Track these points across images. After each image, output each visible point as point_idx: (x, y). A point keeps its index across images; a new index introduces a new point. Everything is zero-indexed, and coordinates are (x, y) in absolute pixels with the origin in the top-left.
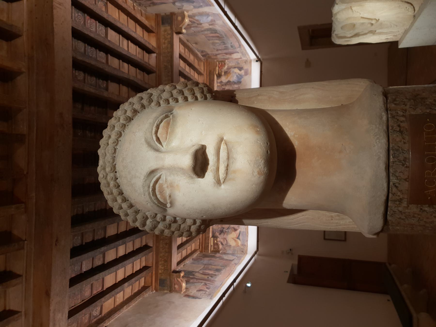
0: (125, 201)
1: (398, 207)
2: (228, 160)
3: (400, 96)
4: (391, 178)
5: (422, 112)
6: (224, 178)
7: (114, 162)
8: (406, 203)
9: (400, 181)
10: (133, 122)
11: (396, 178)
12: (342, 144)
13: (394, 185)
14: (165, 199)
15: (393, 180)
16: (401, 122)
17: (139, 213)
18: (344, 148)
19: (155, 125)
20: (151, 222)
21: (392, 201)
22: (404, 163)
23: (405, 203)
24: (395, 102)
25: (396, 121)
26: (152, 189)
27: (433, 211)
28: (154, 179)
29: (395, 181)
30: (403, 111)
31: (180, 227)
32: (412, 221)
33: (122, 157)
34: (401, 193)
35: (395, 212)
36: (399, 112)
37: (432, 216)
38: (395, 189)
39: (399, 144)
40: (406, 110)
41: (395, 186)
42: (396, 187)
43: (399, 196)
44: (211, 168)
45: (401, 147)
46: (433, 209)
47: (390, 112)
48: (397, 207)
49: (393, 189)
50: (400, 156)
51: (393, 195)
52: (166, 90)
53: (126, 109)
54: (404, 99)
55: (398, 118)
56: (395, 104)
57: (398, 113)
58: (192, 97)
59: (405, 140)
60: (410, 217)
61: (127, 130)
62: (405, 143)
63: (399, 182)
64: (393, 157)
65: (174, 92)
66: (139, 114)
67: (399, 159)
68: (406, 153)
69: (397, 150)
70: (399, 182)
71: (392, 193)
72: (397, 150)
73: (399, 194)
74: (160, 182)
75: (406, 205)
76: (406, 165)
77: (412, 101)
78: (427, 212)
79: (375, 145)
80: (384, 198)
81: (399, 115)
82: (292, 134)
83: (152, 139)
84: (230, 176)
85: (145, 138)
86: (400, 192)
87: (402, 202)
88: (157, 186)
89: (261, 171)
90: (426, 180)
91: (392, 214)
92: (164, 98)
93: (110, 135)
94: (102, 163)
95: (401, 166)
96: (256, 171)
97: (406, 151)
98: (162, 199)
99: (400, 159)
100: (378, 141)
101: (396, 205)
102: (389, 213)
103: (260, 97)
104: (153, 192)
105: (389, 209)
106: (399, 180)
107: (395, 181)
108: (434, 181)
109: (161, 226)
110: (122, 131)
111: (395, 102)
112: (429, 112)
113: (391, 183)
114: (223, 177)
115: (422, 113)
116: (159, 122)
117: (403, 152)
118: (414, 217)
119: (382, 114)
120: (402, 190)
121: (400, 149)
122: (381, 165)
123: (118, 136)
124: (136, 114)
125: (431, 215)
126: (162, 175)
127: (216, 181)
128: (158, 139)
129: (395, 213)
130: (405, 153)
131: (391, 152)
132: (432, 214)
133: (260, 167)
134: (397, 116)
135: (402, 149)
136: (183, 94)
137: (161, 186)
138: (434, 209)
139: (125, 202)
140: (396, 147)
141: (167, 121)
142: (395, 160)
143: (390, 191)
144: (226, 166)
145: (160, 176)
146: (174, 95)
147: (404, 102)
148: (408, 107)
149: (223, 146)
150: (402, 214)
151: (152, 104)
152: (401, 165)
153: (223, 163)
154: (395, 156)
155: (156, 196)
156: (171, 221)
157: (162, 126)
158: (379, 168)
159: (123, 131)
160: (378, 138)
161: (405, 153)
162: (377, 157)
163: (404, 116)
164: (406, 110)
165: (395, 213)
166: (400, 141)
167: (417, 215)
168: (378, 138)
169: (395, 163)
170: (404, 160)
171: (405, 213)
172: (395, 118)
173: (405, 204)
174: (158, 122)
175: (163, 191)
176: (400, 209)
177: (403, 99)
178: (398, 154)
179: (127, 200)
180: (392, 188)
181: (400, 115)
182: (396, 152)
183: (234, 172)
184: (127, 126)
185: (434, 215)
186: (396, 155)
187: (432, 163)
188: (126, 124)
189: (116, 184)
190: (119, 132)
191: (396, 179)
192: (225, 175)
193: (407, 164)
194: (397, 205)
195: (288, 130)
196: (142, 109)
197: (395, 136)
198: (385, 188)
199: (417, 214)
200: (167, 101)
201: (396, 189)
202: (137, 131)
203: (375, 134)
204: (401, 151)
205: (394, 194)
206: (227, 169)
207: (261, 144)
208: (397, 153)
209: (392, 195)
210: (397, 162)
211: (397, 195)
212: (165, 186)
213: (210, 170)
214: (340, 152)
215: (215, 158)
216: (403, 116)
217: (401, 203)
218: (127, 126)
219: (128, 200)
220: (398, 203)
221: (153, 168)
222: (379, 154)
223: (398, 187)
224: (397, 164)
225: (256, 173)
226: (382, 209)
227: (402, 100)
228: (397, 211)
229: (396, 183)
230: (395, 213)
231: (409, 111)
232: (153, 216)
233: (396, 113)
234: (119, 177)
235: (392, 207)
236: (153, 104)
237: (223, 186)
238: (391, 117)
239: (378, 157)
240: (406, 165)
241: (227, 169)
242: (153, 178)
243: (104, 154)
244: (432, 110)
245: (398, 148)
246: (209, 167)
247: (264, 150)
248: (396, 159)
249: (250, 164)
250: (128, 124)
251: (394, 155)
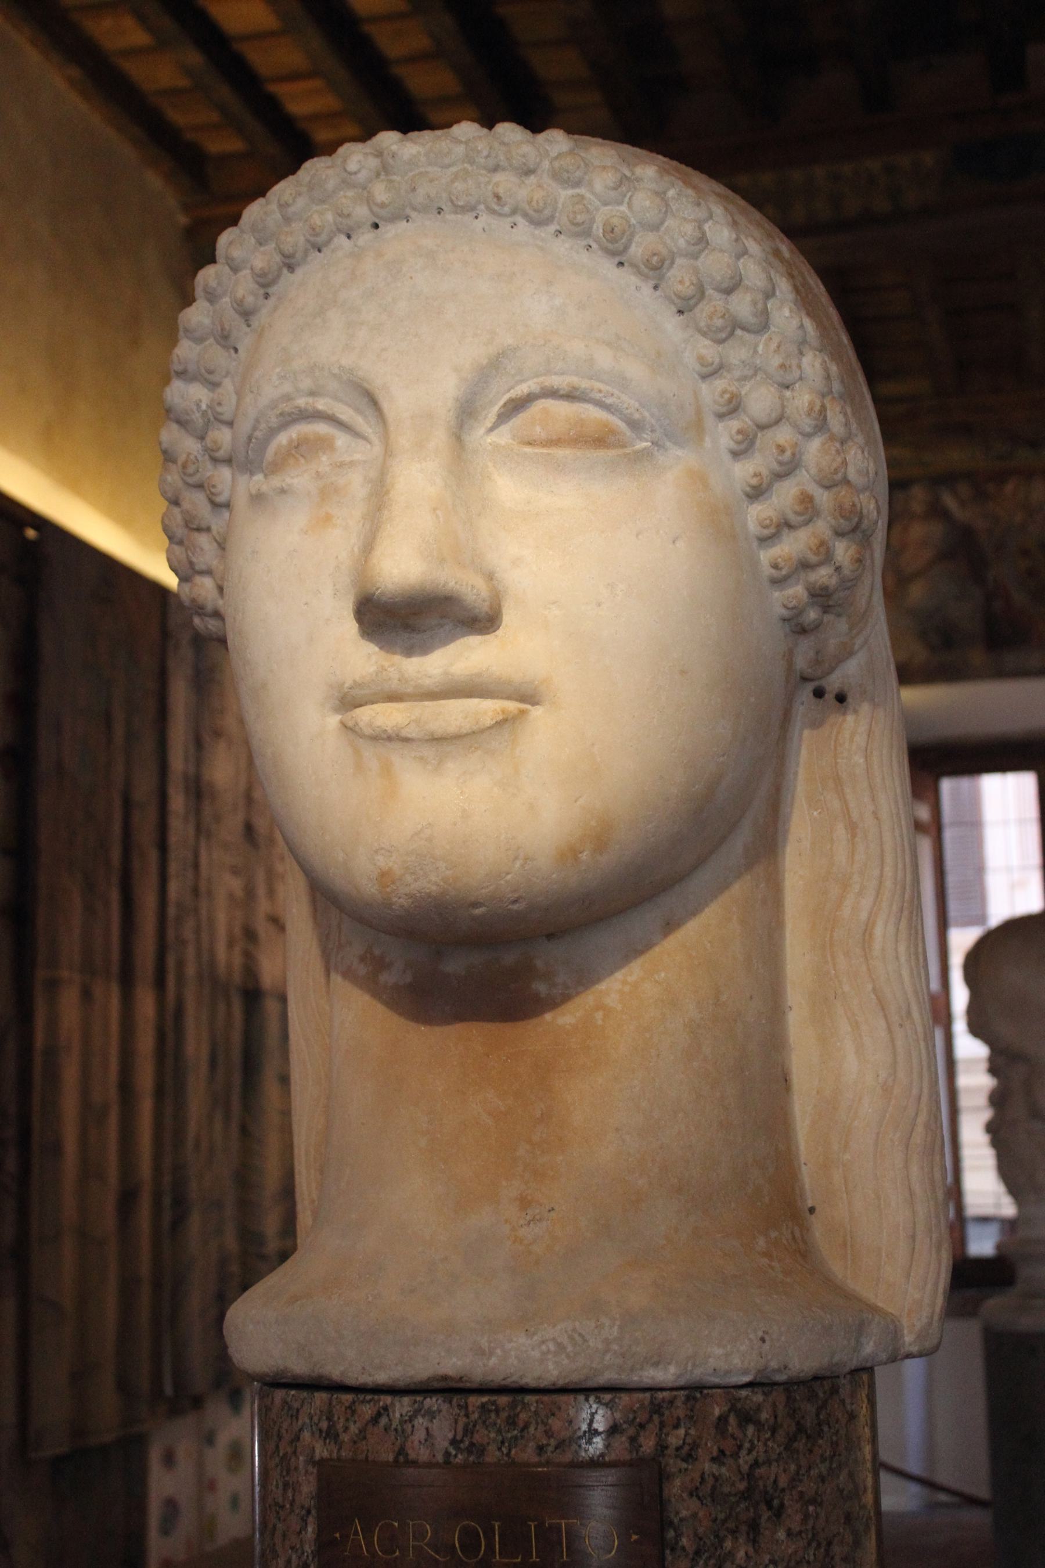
0: (263, 286)
1: (311, 1426)
2: (427, 737)
3: (769, 1439)
4: (406, 1400)
5: (681, 1520)
6: (357, 729)
7: (419, 212)
8: (326, 1454)
9: (396, 1430)
10: (607, 267)
11: (407, 1418)
12: (553, 1209)
13: (382, 1411)
14: (276, 467)
15: (402, 1406)
16: (633, 1440)
17: (225, 347)
18: (538, 1217)
19: (584, 384)
20: (198, 405)
21: (330, 1404)
22: (462, 1445)
23: (325, 1451)
24: (732, 1420)
25: (635, 1418)
26: (306, 410)
27: (306, 1554)
28: (345, 413)
29: (394, 1412)
30: (687, 1448)
31: (199, 530)
32: (275, 1483)
33: (438, 246)
34: (356, 1435)
35: (297, 1419)
36: (682, 1432)
37: (290, 1551)
38: (370, 1412)
39: (536, 1429)
40: (690, 1457)
41: (379, 1415)
42: (375, 1420)
43: (346, 1429)
44: (393, 665)
45: (522, 1437)
46: (310, 1552)
47: (683, 1398)
48: (311, 1422)
49: (368, 1406)
50: (489, 1432)
51: (350, 1407)
52: (788, 393)
53: (666, 224)
54: (748, 1454)
55: (653, 1427)
56: (723, 1419)
57: (676, 1426)
58: (768, 522)
59: (552, 1452)
60: (284, 1473)
61: (562, 247)
62: (541, 1449)
63: (394, 1426)
64: (483, 1406)
65: (784, 435)
66: (647, 289)
67: (478, 1427)
68: (502, 1452)
69: (512, 1422)
70: (394, 1426)
71: (354, 1402)
72: (512, 1422)
73: (354, 1429)
74: (342, 440)
75: (317, 1457)
76: (454, 1452)
77: (742, 1486)
78: (300, 1533)
79: (536, 1338)
80: (335, 1372)
81: (665, 1431)
82: (612, 1001)
83: (517, 378)
84: (369, 753)
85: (516, 349)
86: (360, 1431)
87: (328, 1441)
88: (322, 428)
89: (393, 883)
90: (396, 1524)
91: (290, 1408)
92: (743, 393)
93: (539, 172)
94: (406, 157)
95: (450, 1435)
96: (391, 864)
97: (508, 1454)
98: (276, 454)
99: (478, 1431)
100: (552, 1346)
101: (316, 1419)
102: (293, 1395)
103: (841, 831)
104: (293, 413)
105: (305, 1394)
106: (399, 1428)
107: (397, 1415)
108: (395, 1553)
109: (189, 446)
110: (558, 228)
111: (732, 1420)
112: (680, 1544)
113: (388, 1399)
114: (362, 724)
115: (676, 1521)
116: (598, 396)
117: (503, 1442)
118: (286, 1485)
119: (669, 1364)
120: (365, 1438)
121: (516, 1432)
122: (454, 1360)
123: (531, 212)
124: (646, 277)
125: (292, 1548)
126: (369, 446)
127: (346, 690)
128: (517, 406)
129: (294, 1418)
130: (500, 1449)
131: (503, 1400)
132: (297, 1550)
133: (409, 878)
134: (662, 1425)
135: (516, 1438)
136: (779, 476)
137: (324, 444)
138: (310, 1558)
139: (258, 283)
140: (523, 1416)
141: (613, 432)
142: (473, 1412)
143: (361, 1397)
144: (404, 733)
145: (365, 438)
146: (769, 434)
147: (736, 1455)
148: (708, 1467)
149: (488, 709)
150: (292, 1442)
151: (707, 342)
152: (455, 1436)
153: (413, 717)
154: (490, 1411)
155: (284, 426)
157: (583, 416)
158: (443, 1354)
159: (557, 231)
160: (561, 1347)
161: (500, 1449)
162: (486, 1344)
163: (663, 1451)
164: (690, 1457)
165: (294, 1418)
166: (550, 1433)
167: (291, 1498)
168: (561, 1347)
169: (463, 1413)
170: (472, 1444)
171: (295, 1453)
172: (651, 1416)
173: (321, 1451)
174: (600, 391)
175: (302, 456)
176: (306, 1435)
177: (750, 1451)
178: (495, 1424)
179: (270, 290)
180: (372, 1404)
181: (667, 1435)
182: (504, 1415)
183: (387, 770)
184: (585, 243)
185: (294, 1557)
186: (493, 1415)
187: (457, 1545)
188: (595, 241)
189: (324, 237)
190: (547, 212)
191: (401, 1415)
192: (368, 731)
193: (460, 1456)
194: (317, 1421)
195: (629, 979)
196: (677, 301)
197: (568, 1414)
198: (370, 1375)
199: (293, 1496)
200: (733, 407)
201: (367, 1417)
202: (557, 302)
203: (576, 1336)
204: (509, 1435)
205: (351, 1409)
206: (389, 739)
207: (509, 877)
208: (499, 1421)
209: (347, 1404)
210: (464, 1419)
211: (347, 1420)
212: (324, 461)
213: (386, 664)
214: (524, 1203)
215: (436, 680)
216: (662, 1447)
217: (325, 1439)
218: (585, 243)
219: (267, 296)
220: (324, 1425)
221: (385, 405)
222: (499, 1351)
223: (374, 1425)
224: (456, 1422)
225: (381, 861)
226: (299, 1367)
227: (747, 1445)
228: (300, 1423)
230: (292, 1416)
231: (686, 1470)
232: (221, 414)
233: (679, 1419)
234: (355, 246)
235: (311, 1404)
236: (707, 348)
237: (333, 721)
238: (657, 1402)
239: (487, 1350)
240: (454, 1452)
241: (389, 739)
242: (350, 406)
243: (447, 161)
244: (691, 1556)
245: (521, 1424)
246: (398, 659)
247: (483, 891)
248: (476, 1415)
249: (417, 834)
250: (594, 246)
251: (494, 1408)
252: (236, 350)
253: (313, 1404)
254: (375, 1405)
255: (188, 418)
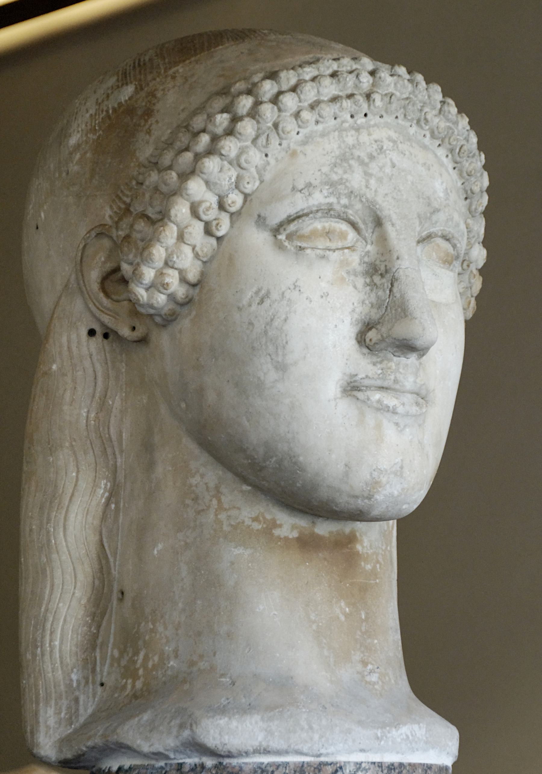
13: (338, 769)
38: (331, 770)
49: (329, 766)
74: (352, 235)
154: (391, 769)
156: (219, 227)
179: (301, 130)
180: (332, 765)
183: (379, 426)
191: (350, 771)
214: (365, 663)
229: (342, 771)
235: (286, 767)
251: (393, 767)
252: (266, 155)
253: (288, 768)
254: (334, 766)
255: (219, 182)
